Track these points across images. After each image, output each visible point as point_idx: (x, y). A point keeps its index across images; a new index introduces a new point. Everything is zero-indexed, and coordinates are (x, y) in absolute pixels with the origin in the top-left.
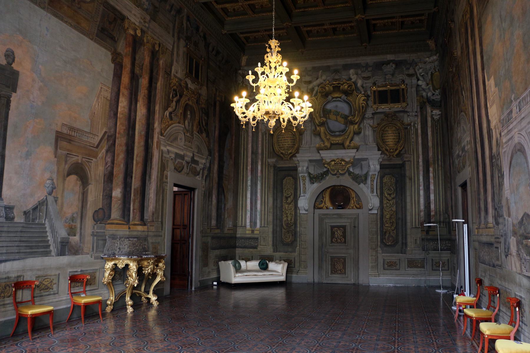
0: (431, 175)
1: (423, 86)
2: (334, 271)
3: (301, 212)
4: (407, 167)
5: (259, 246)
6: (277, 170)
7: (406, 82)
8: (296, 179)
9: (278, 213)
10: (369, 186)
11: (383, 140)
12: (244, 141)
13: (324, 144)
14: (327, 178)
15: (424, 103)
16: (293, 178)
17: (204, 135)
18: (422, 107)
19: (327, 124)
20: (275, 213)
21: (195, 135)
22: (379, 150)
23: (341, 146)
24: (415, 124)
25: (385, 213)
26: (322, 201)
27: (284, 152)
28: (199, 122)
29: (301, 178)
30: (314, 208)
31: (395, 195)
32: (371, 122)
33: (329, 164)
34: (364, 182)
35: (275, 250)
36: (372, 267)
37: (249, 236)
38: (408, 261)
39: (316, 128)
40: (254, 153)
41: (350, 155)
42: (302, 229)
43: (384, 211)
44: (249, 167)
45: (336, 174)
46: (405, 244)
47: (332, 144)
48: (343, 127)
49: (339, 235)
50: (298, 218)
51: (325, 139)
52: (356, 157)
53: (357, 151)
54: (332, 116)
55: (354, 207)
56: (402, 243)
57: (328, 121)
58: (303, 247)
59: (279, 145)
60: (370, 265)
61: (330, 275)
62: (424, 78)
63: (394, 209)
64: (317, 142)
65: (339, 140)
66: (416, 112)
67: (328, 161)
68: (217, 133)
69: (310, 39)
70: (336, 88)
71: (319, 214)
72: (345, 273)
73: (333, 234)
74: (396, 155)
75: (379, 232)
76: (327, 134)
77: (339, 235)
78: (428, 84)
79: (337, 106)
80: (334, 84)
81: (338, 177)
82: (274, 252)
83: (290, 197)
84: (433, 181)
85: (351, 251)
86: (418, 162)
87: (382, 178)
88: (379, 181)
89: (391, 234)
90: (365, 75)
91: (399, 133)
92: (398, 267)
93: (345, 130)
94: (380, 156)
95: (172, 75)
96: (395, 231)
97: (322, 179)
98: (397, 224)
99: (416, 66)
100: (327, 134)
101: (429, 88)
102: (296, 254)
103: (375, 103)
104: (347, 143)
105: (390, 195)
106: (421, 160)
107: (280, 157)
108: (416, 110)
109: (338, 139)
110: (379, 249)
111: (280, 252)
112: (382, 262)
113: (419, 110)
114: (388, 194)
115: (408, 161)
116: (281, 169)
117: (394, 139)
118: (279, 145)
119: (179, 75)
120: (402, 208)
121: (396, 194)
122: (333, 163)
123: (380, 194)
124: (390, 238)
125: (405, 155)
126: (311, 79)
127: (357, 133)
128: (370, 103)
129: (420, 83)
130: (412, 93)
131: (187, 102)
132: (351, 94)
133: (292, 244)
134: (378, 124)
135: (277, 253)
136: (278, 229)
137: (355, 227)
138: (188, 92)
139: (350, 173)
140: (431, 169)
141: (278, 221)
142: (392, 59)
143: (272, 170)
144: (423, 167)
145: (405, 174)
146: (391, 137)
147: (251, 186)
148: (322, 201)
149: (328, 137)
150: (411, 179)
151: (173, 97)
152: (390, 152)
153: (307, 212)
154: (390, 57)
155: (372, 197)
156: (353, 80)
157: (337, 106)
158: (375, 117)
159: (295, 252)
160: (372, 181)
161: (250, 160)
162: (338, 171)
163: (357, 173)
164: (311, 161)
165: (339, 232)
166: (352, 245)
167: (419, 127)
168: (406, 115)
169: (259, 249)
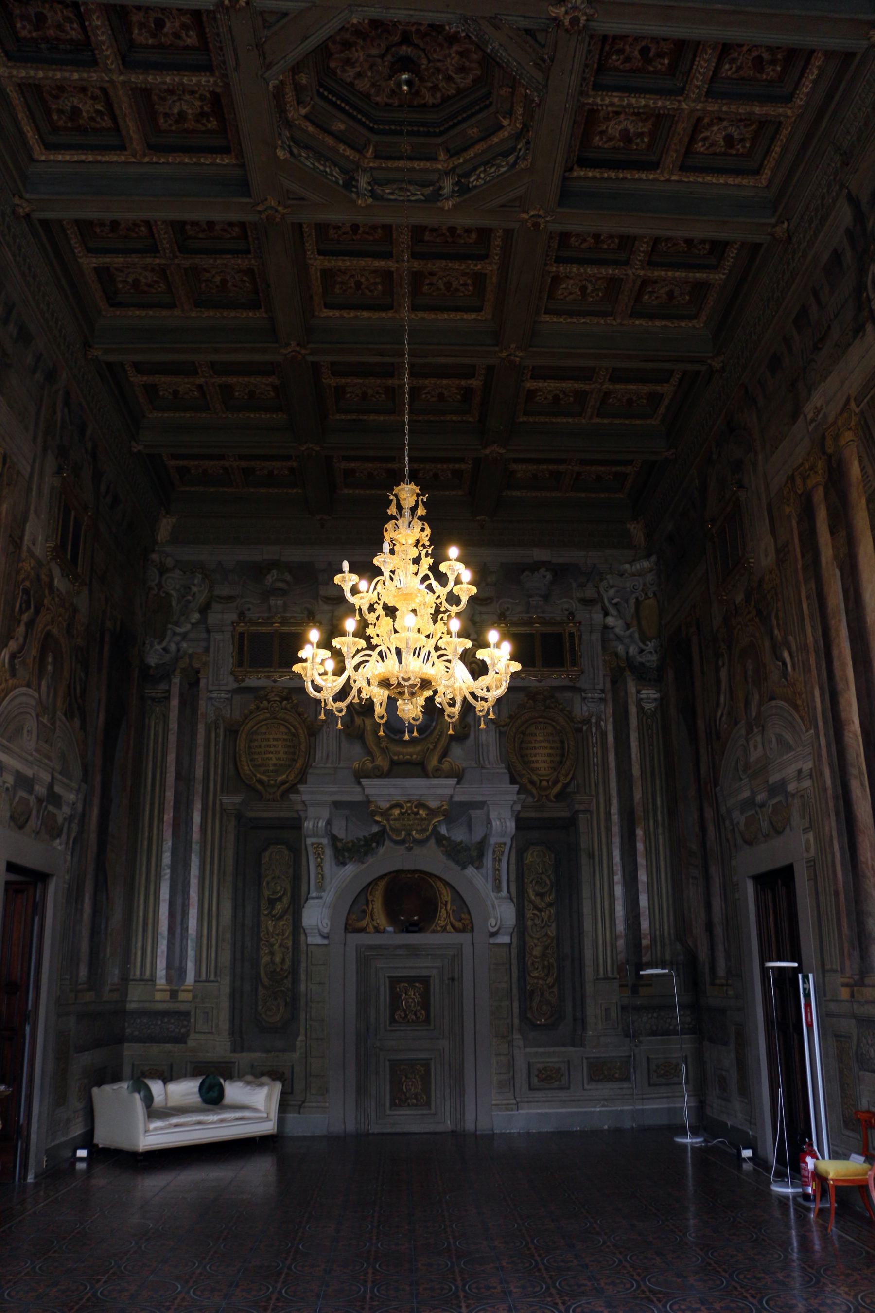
0: (640, 846)
1: (617, 630)
2: (399, 1099)
3: (311, 940)
5: (192, 1036)
7: (578, 617)
8: (296, 851)
10: (490, 872)
11: (522, 756)
12: (156, 742)
13: (373, 761)
14: (382, 850)
15: (621, 670)
17: (77, 722)
18: (616, 681)
21: (58, 723)
22: (513, 781)
24: (599, 719)
26: (364, 912)
27: (264, 778)
28: (69, 687)
29: (311, 851)
30: (346, 929)
31: (553, 896)
33: (385, 814)
35: (239, 1045)
37: (164, 1006)
40: (184, 777)
41: (439, 791)
43: (527, 938)
44: (168, 816)
45: (403, 842)
46: (581, 1022)
47: (393, 763)
49: (412, 1001)
50: (303, 958)
51: (375, 749)
52: (457, 799)
53: (458, 783)
55: (449, 927)
56: (575, 1020)
61: (388, 1112)
62: (619, 611)
63: (552, 931)
66: (603, 691)
67: (384, 805)
68: (102, 716)
69: (346, 491)
72: (428, 1104)
73: (395, 998)
74: (556, 796)
78: (628, 626)
81: (410, 849)
82: (234, 1051)
83: (280, 899)
84: (644, 862)
86: (608, 814)
87: (520, 853)
88: (513, 860)
89: (545, 995)
91: (562, 742)
94: (515, 798)
95: (25, 548)
96: (555, 989)
97: (366, 854)
99: (601, 580)
101: (631, 636)
102: (297, 1055)
104: (434, 762)
105: (542, 895)
106: (614, 809)
108: (601, 686)
110: (517, 1036)
113: (608, 686)
114: (538, 894)
117: (549, 755)
118: (251, 760)
119: (38, 551)
122: (396, 812)
129: (610, 621)
131: (48, 628)
134: (511, 717)
135: (244, 1054)
137: (454, 980)
138: (53, 599)
139: (440, 840)
140: (639, 832)
142: (544, 558)
144: (621, 827)
146: (541, 751)
147: (173, 867)
150: (591, 856)
151: (21, 612)
153: (325, 942)
154: (540, 554)
155: (496, 902)
160: (497, 860)
161: (170, 795)
163: (459, 840)
164: (337, 805)
165: (411, 993)
167: (610, 728)
169: (191, 1043)
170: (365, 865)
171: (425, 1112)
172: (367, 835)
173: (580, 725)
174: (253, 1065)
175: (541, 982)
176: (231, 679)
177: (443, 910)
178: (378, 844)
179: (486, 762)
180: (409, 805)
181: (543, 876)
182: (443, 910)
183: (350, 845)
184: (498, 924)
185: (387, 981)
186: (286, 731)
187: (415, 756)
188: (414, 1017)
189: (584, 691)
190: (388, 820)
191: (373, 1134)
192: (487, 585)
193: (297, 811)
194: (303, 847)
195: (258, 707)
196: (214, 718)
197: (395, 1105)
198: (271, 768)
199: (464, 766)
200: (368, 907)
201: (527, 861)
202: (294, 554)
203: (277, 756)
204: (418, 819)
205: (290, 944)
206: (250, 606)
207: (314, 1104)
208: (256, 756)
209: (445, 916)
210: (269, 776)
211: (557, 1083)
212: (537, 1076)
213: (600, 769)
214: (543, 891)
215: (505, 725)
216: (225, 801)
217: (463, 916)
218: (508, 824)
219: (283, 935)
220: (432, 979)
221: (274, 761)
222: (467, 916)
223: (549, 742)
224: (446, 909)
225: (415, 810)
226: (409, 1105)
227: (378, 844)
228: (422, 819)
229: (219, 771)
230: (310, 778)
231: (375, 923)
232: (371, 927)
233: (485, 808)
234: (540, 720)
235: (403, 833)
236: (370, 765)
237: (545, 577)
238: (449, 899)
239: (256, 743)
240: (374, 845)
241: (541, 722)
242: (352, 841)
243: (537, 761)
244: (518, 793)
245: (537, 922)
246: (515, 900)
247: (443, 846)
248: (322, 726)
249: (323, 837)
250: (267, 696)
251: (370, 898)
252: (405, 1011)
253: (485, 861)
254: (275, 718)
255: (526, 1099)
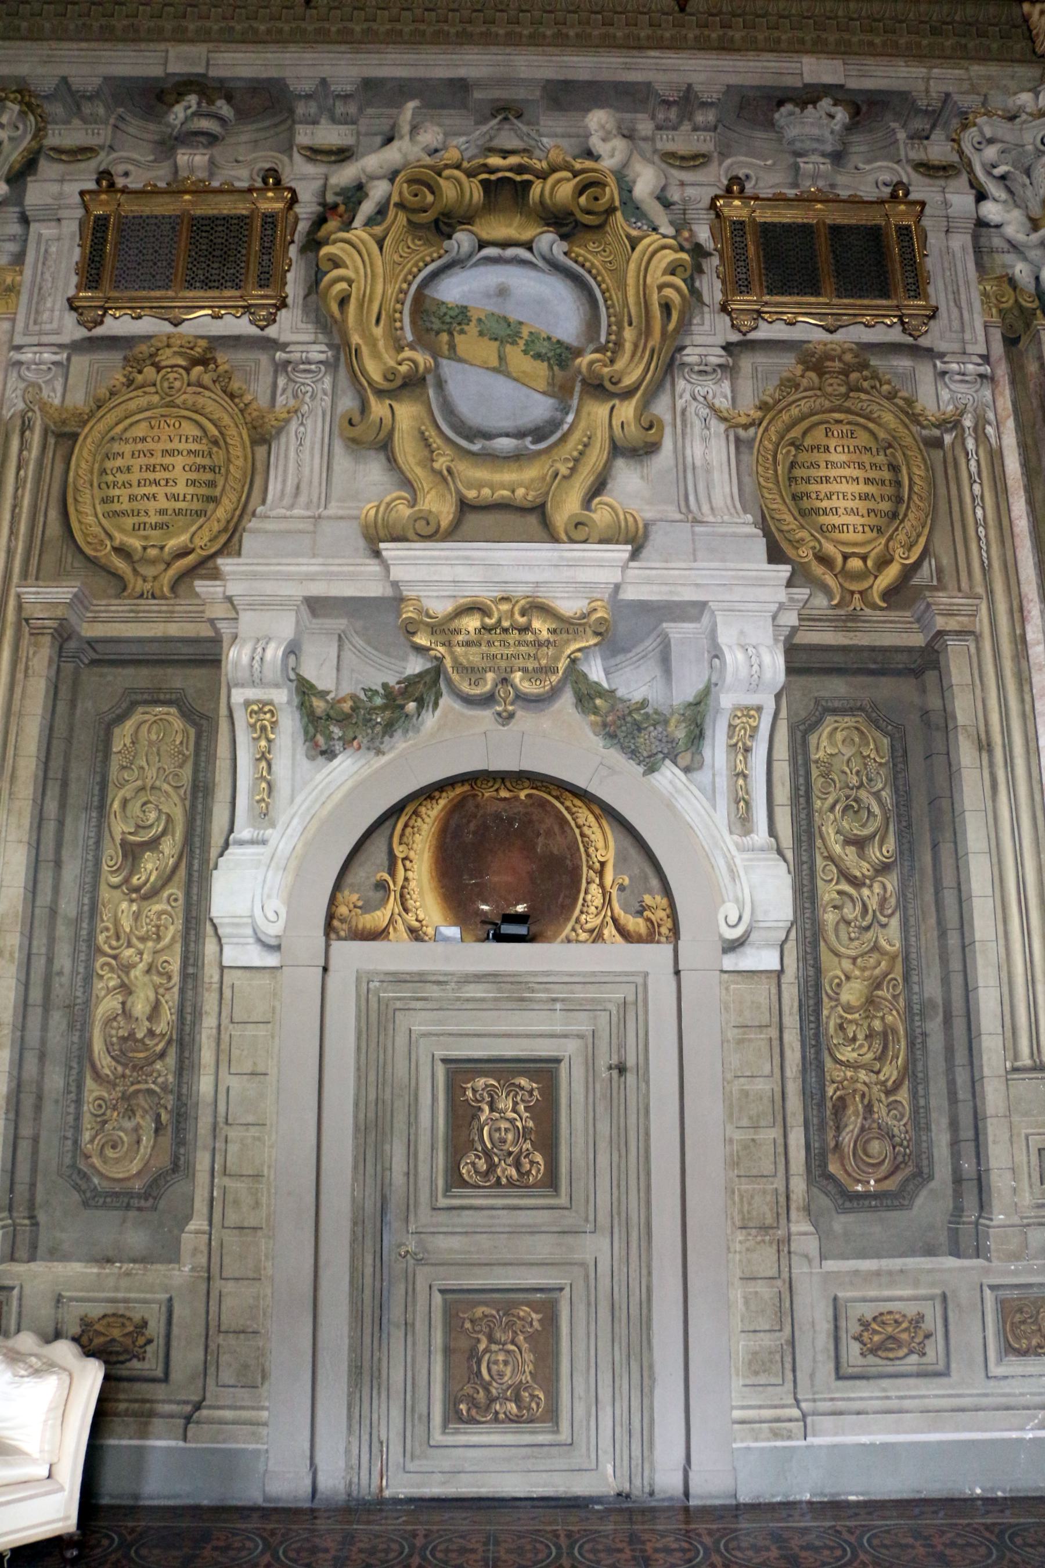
1: (1010, 231)
2: (469, 1402)
4: (958, 671)
6: (78, 658)
8: (203, 722)
9: (63, 961)
10: (722, 783)
11: (794, 497)
13: (413, 503)
14: (430, 720)
16: (189, 714)
19: (440, 385)
20: (39, 965)
22: (775, 555)
23: (533, 520)
25: (833, 969)
26: (382, 886)
30: (329, 928)
31: (891, 845)
32: (720, 392)
34: (685, 759)
36: (757, 1364)
38: (1004, 1308)
39: (364, 408)
42: (234, 1082)
43: (826, 958)
47: (465, 507)
48: (539, 408)
50: (210, 1002)
51: (418, 473)
52: (629, 594)
53: (635, 555)
54: (467, 342)
55: (609, 931)
56: (958, 1180)
57: (449, 369)
58: (232, 1218)
59: (105, 500)
60: (742, 1345)
61: (437, 1437)
62: (1010, 192)
64: (368, 484)
65: (517, 482)
66: (986, 359)
67: (441, 608)
70: (506, 192)
71: (363, 979)
72: (552, 1415)
73: (462, 1117)
74: (888, 594)
75: (795, 1103)
76: (437, 441)
77: (506, 1125)
79: (503, 292)
80: (492, 171)
81: (507, 718)
83: (153, 844)
85: (596, 1247)
87: (801, 733)
88: (782, 751)
90: (683, 142)
91: (894, 468)
92: (934, 1351)
93: (554, 425)
96: (903, 1095)
97: (389, 728)
98: (916, 1042)
100: (437, 441)
102: (181, 1274)
103: (743, 286)
104: (568, 506)
105: (860, 844)
107: (107, 574)
109: (508, 476)
110: (800, 1225)
111: (55, 1254)
112: (825, 1326)
113: (998, 348)
114: (848, 842)
115: (958, 633)
116: (107, 656)
117: (865, 497)
118: (105, 500)
120: (943, 934)
121: (900, 836)
122: (472, 623)
123: (797, 839)
124: (875, 1146)
125: (942, 599)
126: (348, 141)
127: (642, 450)
128: (712, 289)
129: (991, 210)
130: (946, 254)
132: (600, 227)
133: (154, 1196)
134: (764, 407)
135: (35, 1267)
136: (55, 1080)
139: (587, 696)
141: (58, 1019)
142: (828, 79)
143: (41, 658)
145: (948, 716)
146: (844, 487)
148: (382, 886)
149: (441, 463)
150: (985, 746)
152: (845, 574)
153: (271, 960)
154: (817, 69)
155: (739, 859)
156: (607, 163)
157: (503, 292)
158: (746, 363)
159: (172, 1255)
162: (505, 681)
163: (637, 696)
164: (316, 606)
165: (505, 1103)
166: (603, 1199)
168: (925, 372)
170: (383, 760)
171: (540, 1438)
172: (392, 681)
173: (937, 432)
174: (59, 1300)
175: (862, 1075)
176: (70, 319)
177: (594, 888)
178: (421, 702)
179: (706, 508)
180: (505, 607)
181: (863, 794)
182: (594, 888)
183: (347, 706)
184: (746, 918)
185: (441, 1070)
186: (198, 432)
187: (520, 492)
188: (513, 1172)
189: (941, 356)
190: (448, 644)
191: (396, 1501)
192: (695, 129)
193: (212, 621)
194: (223, 711)
195: (130, 382)
196: (21, 406)
197: (460, 1420)
198: (154, 519)
199: (649, 515)
200: (392, 871)
201: (821, 754)
202: (240, 63)
203: (169, 490)
204: (527, 644)
205: (175, 967)
206: (130, 167)
207: (228, 1414)
208: (117, 492)
209: (598, 901)
210: (146, 538)
211: (914, 1358)
212: (858, 1338)
213: (993, 534)
214: (866, 832)
215: (752, 424)
216: (31, 598)
217: (648, 899)
218: (767, 659)
219: (159, 938)
220: (563, 1067)
221: (163, 503)
222: (661, 901)
223: (861, 466)
224: (602, 885)
225: (522, 620)
226: (496, 1420)
227: (421, 702)
228: (539, 644)
229: (23, 528)
230: (249, 542)
231: (411, 918)
232: (401, 927)
233: (705, 619)
234: (837, 416)
235: (490, 676)
236: (404, 511)
237: (832, 116)
238: (610, 857)
239: (119, 462)
240: (412, 706)
241: (839, 422)
242: (354, 697)
243: (835, 511)
244: (790, 584)
245: (850, 912)
246: (789, 855)
247: (596, 711)
248: (287, 421)
249: (277, 686)
250: (156, 354)
251: (399, 851)
252: (488, 1154)
253: (707, 752)
254: (171, 405)
255: (826, 1406)
